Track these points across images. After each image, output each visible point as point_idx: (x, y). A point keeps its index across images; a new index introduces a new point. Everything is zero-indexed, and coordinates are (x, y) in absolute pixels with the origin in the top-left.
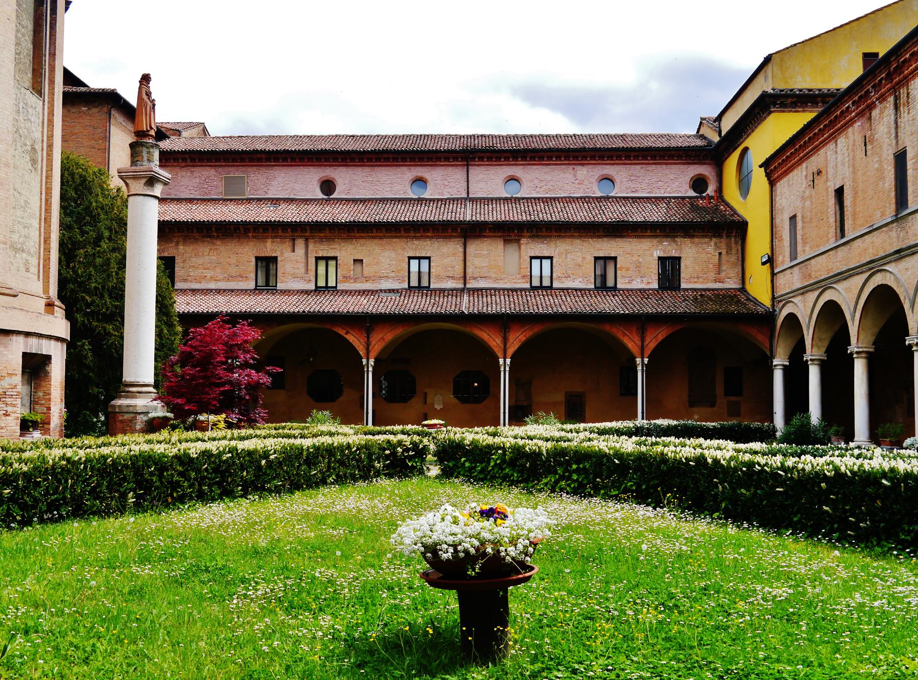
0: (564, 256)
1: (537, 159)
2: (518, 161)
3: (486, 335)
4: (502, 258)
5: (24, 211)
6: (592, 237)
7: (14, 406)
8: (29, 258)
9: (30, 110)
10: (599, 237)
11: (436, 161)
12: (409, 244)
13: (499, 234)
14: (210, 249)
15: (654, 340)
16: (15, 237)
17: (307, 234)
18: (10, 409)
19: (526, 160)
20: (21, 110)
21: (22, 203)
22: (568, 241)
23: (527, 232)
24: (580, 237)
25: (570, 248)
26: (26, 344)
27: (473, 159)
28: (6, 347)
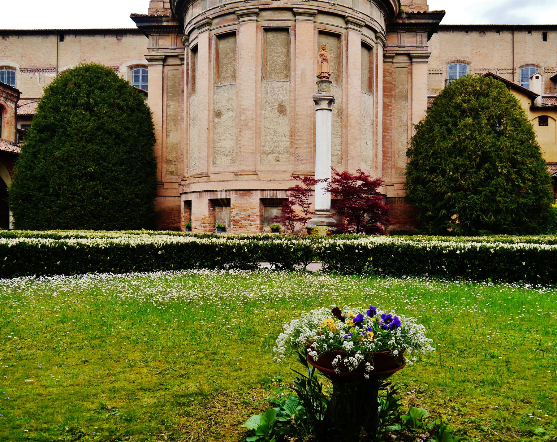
5: (273, 136)
7: (255, 221)
8: (280, 156)
9: (277, 90)
16: (267, 148)
18: (252, 223)
20: (269, 92)
21: (272, 132)
26: (262, 195)
28: (249, 197)
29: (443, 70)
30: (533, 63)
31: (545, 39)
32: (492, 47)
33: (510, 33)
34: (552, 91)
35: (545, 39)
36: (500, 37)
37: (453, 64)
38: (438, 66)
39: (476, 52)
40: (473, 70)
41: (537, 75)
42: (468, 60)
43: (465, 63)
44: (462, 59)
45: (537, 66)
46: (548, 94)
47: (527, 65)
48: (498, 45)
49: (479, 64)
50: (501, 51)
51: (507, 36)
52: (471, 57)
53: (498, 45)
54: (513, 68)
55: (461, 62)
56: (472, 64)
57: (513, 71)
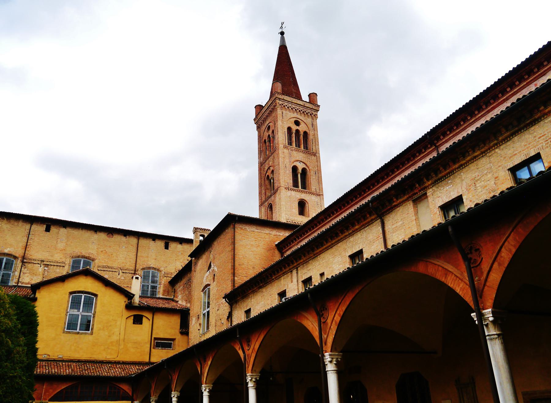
0: (473, 188)
1: (492, 101)
2: (476, 115)
3: (310, 324)
4: (414, 222)
6: (498, 145)
10: (506, 140)
11: (414, 159)
12: (348, 244)
13: (406, 197)
14: (262, 297)
15: (496, 265)
17: (295, 264)
19: (483, 110)
22: (472, 166)
23: (428, 180)
24: (484, 154)
25: (476, 174)
27: (438, 139)
29: (66, 263)
30: (154, 266)
31: (167, 247)
32: (118, 248)
33: (136, 238)
34: (170, 293)
35: (167, 247)
36: (127, 241)
37: (78, 259)
38: (61, 258)
39: (102, 250)
40: (96, 267)
41: (137, 276)
42: (92, 257)
43: (90, 259)
44: (87, 255)
45: (158, 270)
46: (166, 296)
47: (149, 268)
48: (124, 247)
49: (103, 261)
50: (126, 253)
51: (133, 240)
52: (96, 255)
53: (124, 247)
54: (135, 269)
55: (86, 258)
56: (96, 261)
57: (135, 272)
